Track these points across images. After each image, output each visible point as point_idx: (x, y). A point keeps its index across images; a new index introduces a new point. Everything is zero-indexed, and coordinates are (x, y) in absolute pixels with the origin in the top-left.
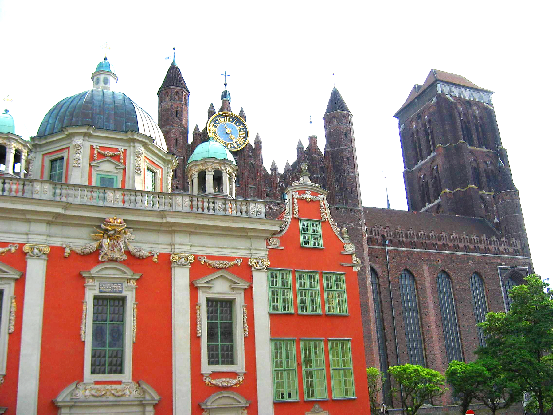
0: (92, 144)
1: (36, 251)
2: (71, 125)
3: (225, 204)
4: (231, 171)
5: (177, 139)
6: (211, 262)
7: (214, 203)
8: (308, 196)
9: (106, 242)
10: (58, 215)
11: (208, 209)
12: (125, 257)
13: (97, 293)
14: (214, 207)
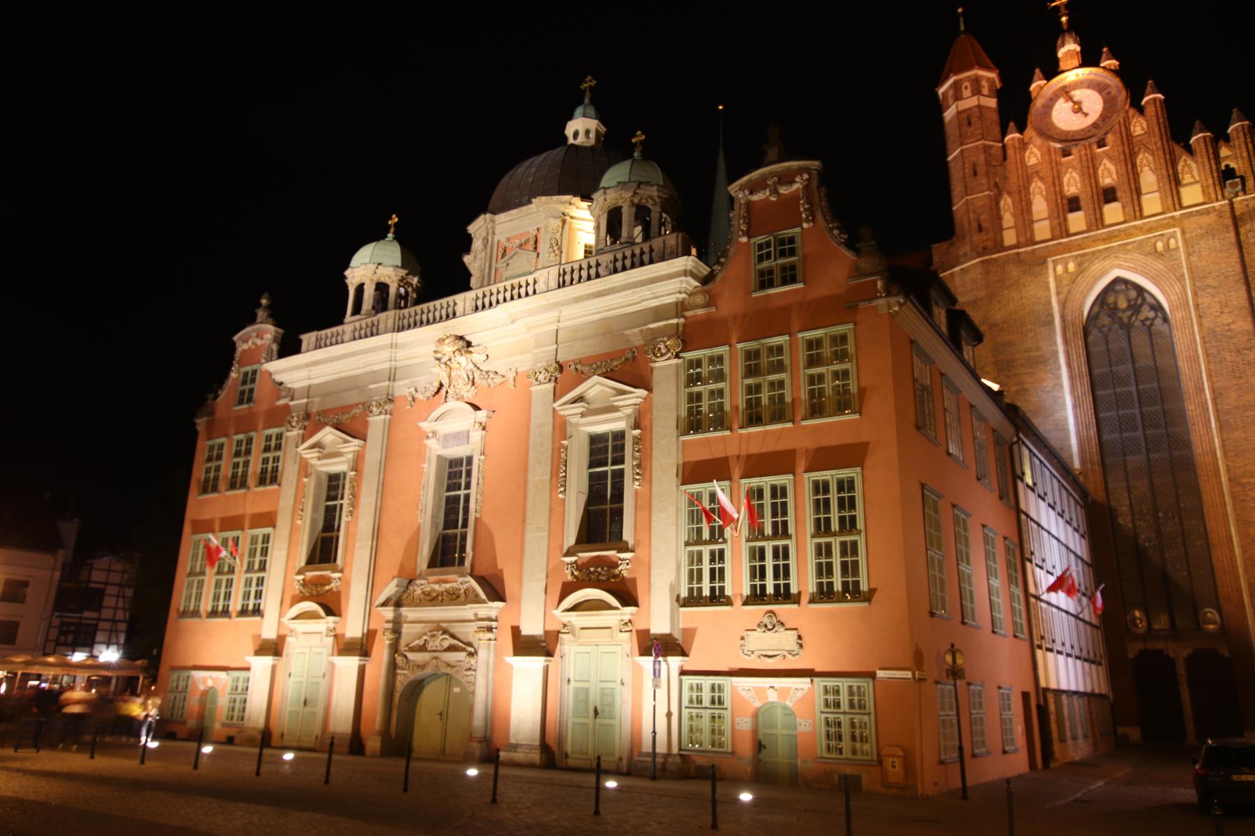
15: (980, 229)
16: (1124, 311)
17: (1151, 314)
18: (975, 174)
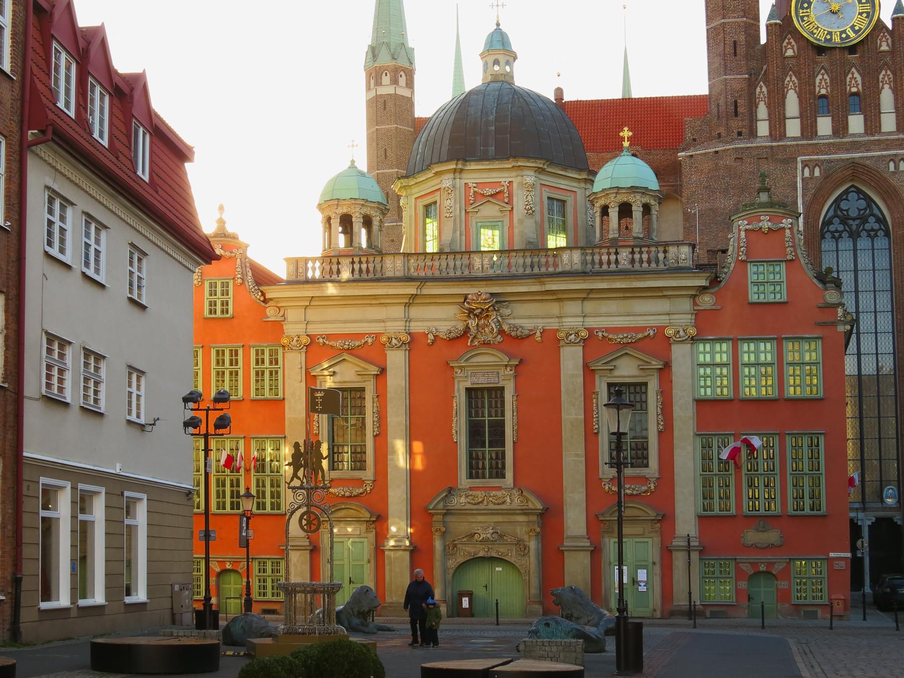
0: (466, 181)
1: (394, 341)
2: (440, 162)
3: (633, 253)
4: (646, 200)
5: (735, 42)
6: (610, 336)
7: (617, 253)
8: (766, 224)
9: (473, 323)
10: (413, 297)
11: (609, 263)
12: (499, 338)
13: (469, 385)
14: (617, 259)
15: (736, 114)
16: (854, 219)
17: (876, 226)
18: (735, 54)
